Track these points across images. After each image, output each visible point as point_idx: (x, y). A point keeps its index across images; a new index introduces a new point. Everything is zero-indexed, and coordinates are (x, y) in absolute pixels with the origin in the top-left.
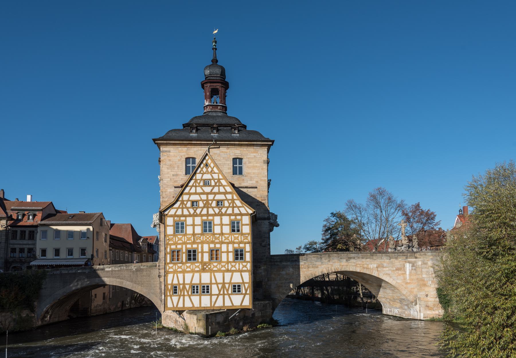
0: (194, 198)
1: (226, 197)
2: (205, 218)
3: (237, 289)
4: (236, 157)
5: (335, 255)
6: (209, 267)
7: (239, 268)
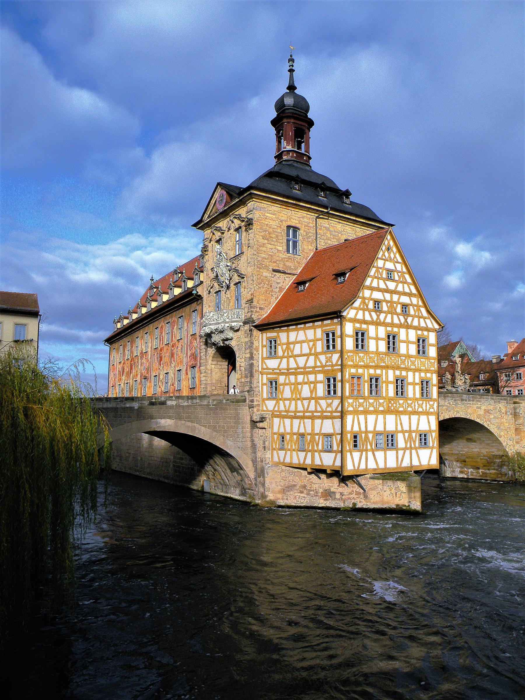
1: (411, 299)
5: (450, 395)
6: (395, 405)
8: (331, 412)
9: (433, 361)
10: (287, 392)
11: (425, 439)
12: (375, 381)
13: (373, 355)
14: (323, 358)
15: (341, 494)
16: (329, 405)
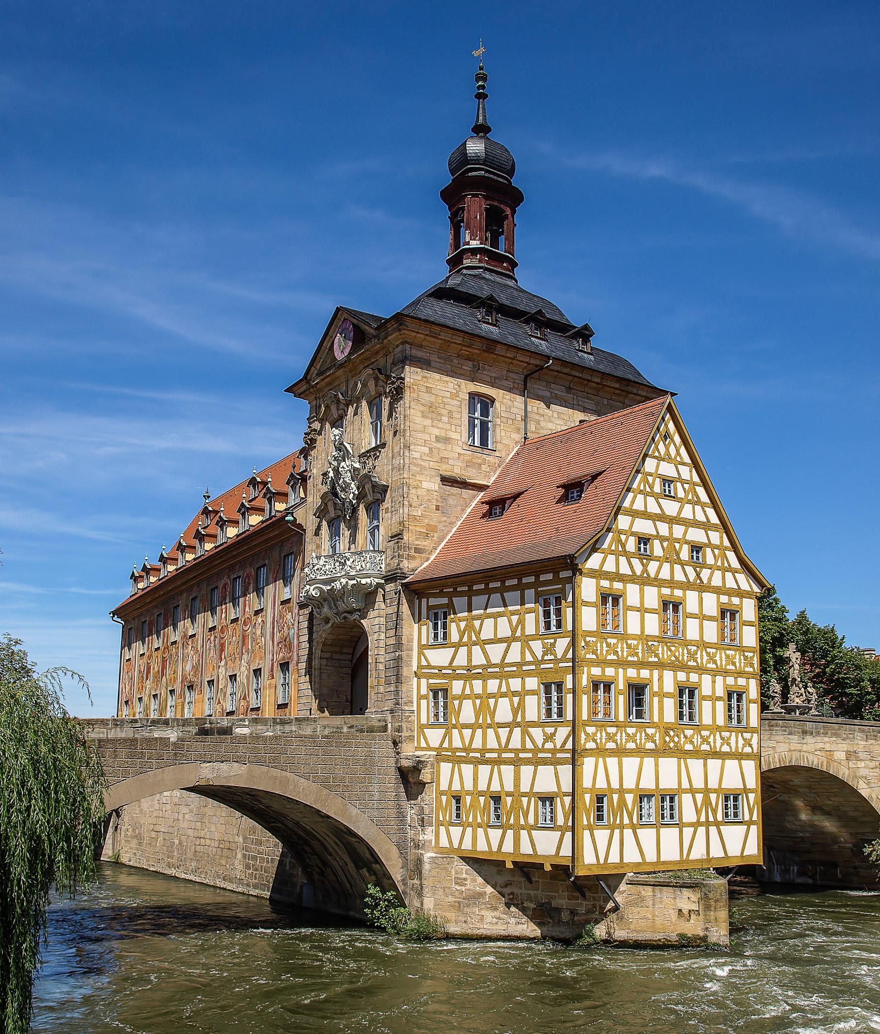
0: (644, 527)
2: (666, 591)
6: (676, 739)
7: (737, 747)
8: (554, 751)
9: (751, 654)
10: (467, 713)
11: (736, 807)
12: (637, 692)
13: (635, 642)
14: (537, 647)
15: (573, 913)
16: (550, 738)
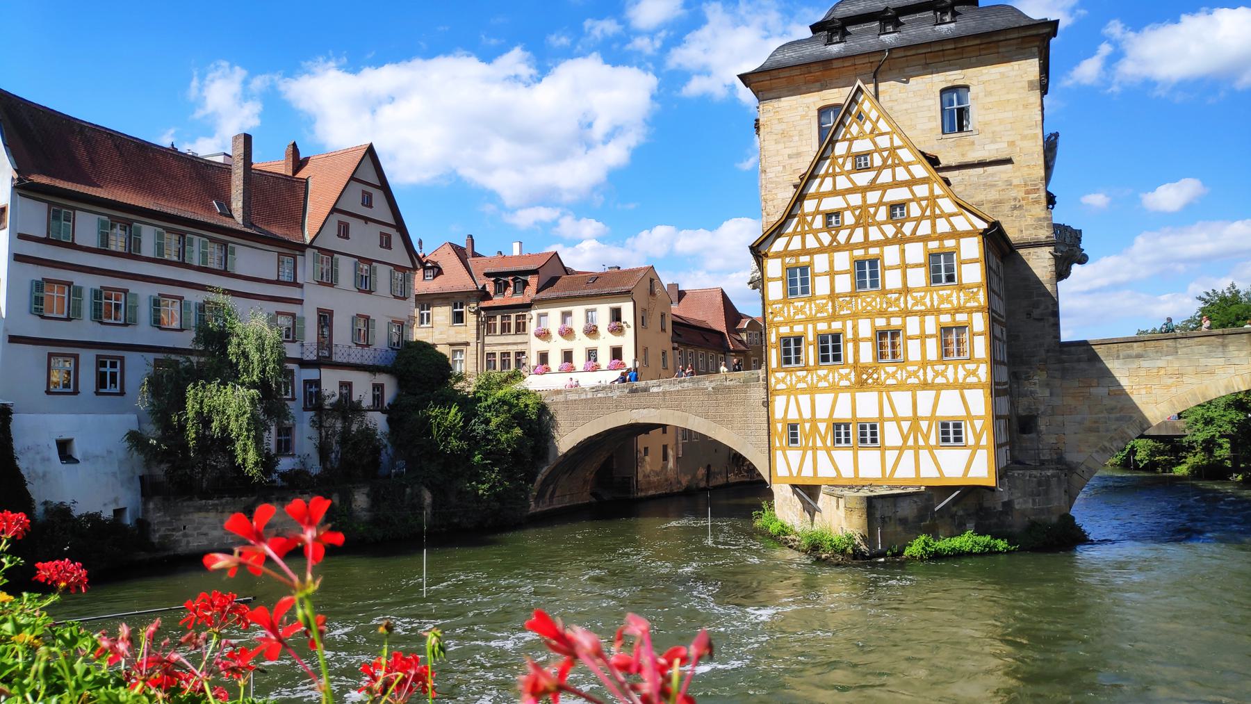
0: (830, 204)
1: (912, 191)
2: (859, 253)
3: (951, 433)
4: (950, 85)
6: (875, 376)
7: (956, 379)
